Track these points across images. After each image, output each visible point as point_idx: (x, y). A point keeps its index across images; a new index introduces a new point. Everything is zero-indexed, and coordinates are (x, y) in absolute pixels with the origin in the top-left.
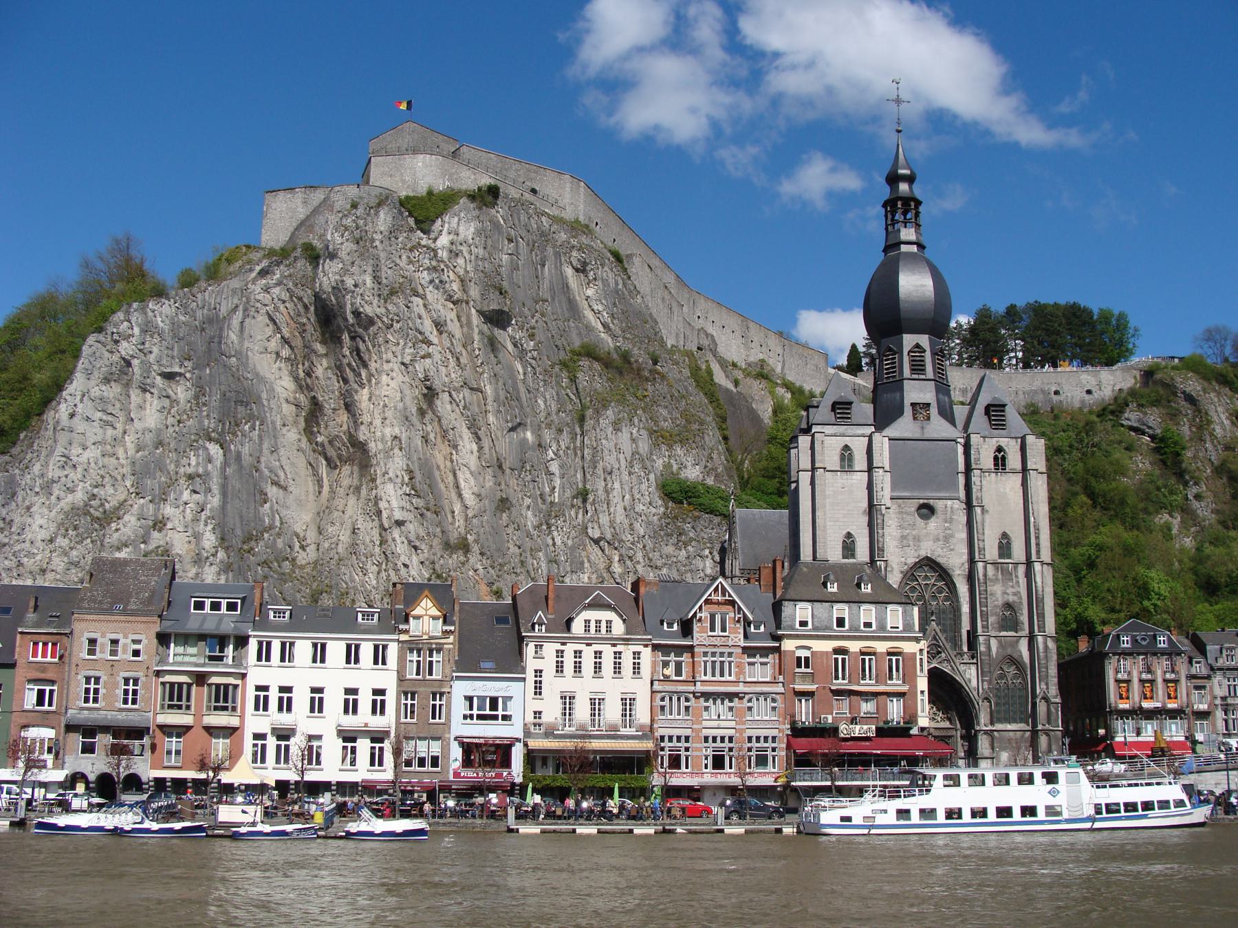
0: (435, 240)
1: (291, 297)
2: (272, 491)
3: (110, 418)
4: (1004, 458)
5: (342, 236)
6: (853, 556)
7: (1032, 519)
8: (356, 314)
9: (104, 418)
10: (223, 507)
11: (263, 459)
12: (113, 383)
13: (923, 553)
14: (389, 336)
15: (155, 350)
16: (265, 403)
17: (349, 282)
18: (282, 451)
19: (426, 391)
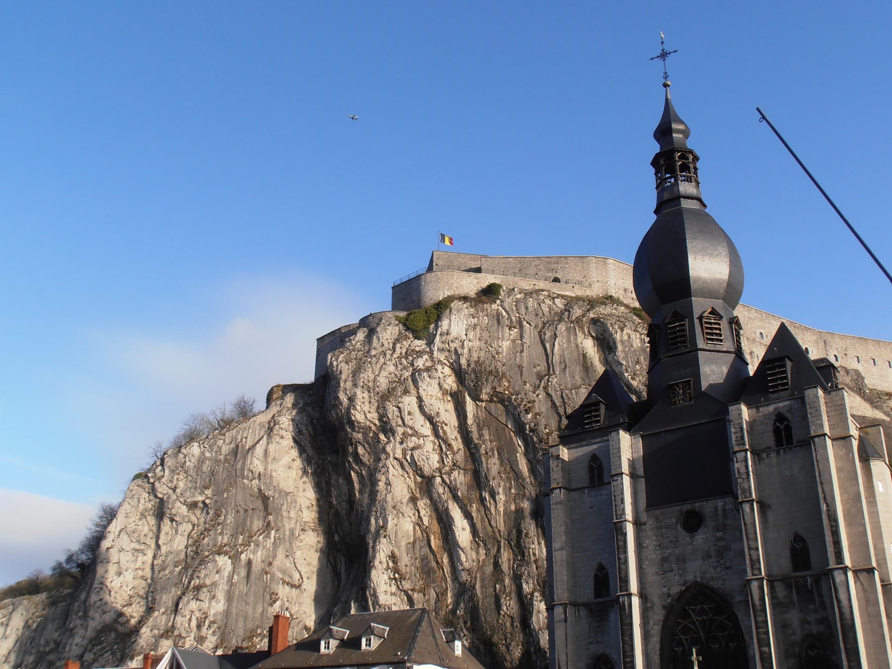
0: (430, 342)
1: (312, 420)
2: (283, 591)
3: (142, 547)
4: (788, 429)
5: (337, 360)
6: (608, 593)
7: (824, 507)
8: (351, 423)
9: (137, 546)
10: (227, 613)
11: (276, 563)
12: (149, 518)
13: (690, 577)
14: (382, 437)
15: (181, 484)
16: (285, 514)
17: (343, 397)
18: (298, 554)
19: (419, 479)
